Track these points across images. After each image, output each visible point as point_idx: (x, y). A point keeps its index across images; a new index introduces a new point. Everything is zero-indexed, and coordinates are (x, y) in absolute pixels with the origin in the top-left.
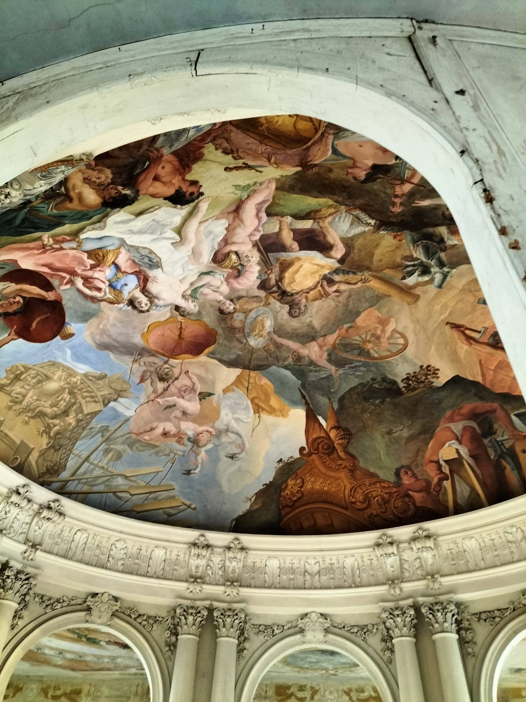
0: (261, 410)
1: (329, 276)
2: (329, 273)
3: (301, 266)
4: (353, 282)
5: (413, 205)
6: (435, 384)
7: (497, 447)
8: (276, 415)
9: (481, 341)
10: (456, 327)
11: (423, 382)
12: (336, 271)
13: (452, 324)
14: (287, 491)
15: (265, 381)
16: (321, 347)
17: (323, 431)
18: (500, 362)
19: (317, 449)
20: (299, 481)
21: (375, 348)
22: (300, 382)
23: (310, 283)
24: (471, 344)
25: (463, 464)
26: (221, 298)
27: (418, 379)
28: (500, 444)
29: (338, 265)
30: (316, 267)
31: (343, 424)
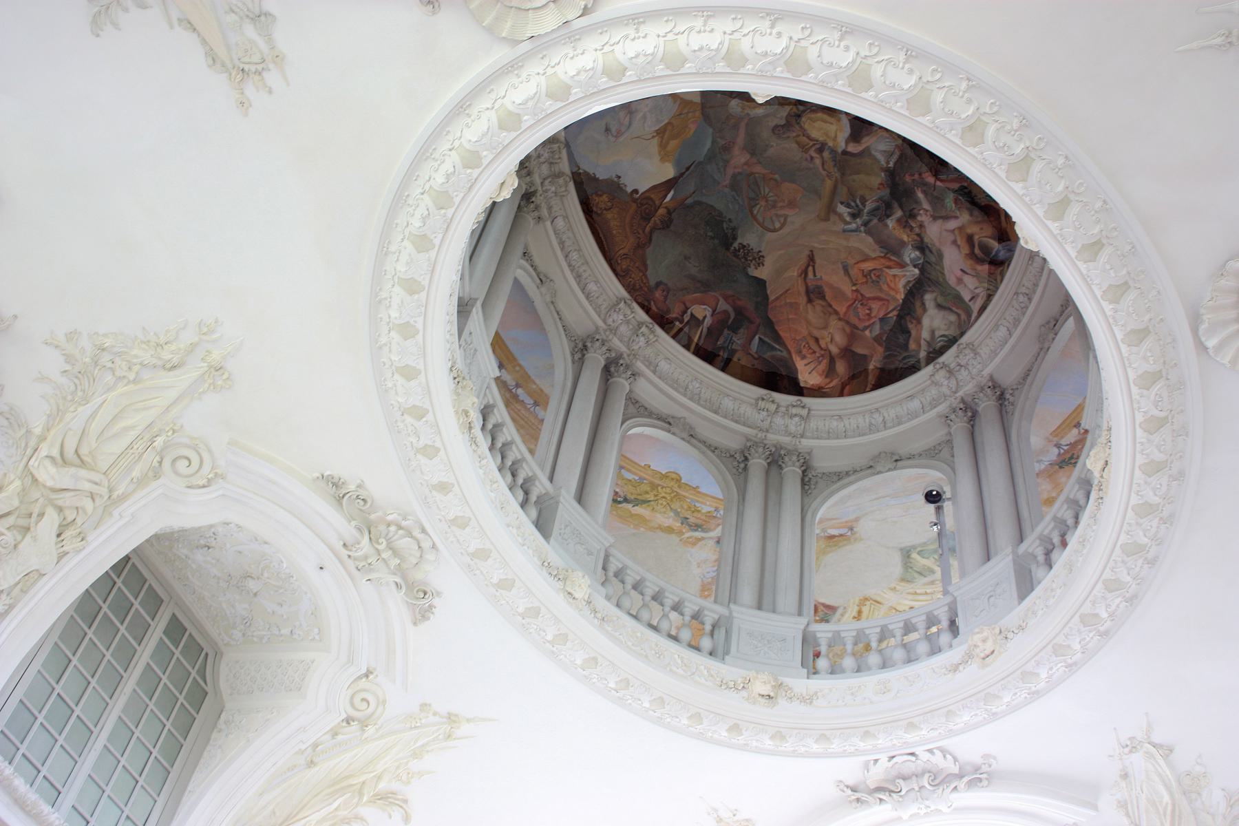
0: (661, 135)
1: (827, 147)
2: (829, 147)
3: (832, 124)
4: (826, 167)
5: (916, 188)
6: (749, 269)
7: (728, 341)
8: (660, 152)
9: (808, 281)
10: (811, 259)
11: (746, 260)
12: (833, 151)
13: (813, 255)
14: (597, 198)
15: (693, 128)
16: (746, 164)
17: (661, 201)
18: (796, 303)
19: (642, 204)
20: (609, 204)
21: (762, 208)
22: (702, 160)
23: (815, 134)
24: (801, 276)
25: (699, 327)
27: (748, 255)
28: (731, 342)
29: (840, 151)
30: (833, 135)
31: (674, 215)
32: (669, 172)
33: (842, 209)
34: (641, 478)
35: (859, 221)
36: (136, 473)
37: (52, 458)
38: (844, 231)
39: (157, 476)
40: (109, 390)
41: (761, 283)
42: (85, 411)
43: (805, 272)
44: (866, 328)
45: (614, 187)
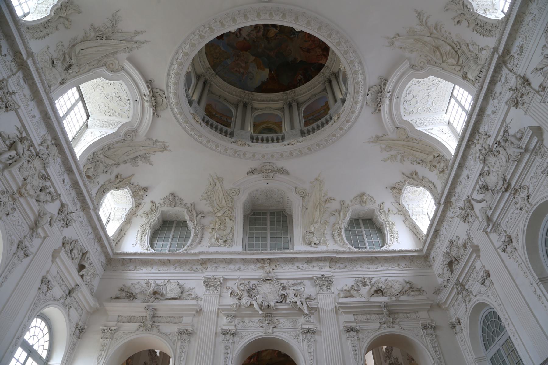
10: (301, 48)
23: (273, 35)
26: (254, 37)
29: (278, 32)
32: (267, 70)
33: (292, 36)
34: (324, 110)
35: (296, 34)
36: (230, 202)
37: (218, 212)
38: (297, 38)
39: (233, 199)
40: (214, 196)
41: (301, 61)
42: (215, 202)
43: (303, 50)
44: (320, 43)
45: (263, 83)
